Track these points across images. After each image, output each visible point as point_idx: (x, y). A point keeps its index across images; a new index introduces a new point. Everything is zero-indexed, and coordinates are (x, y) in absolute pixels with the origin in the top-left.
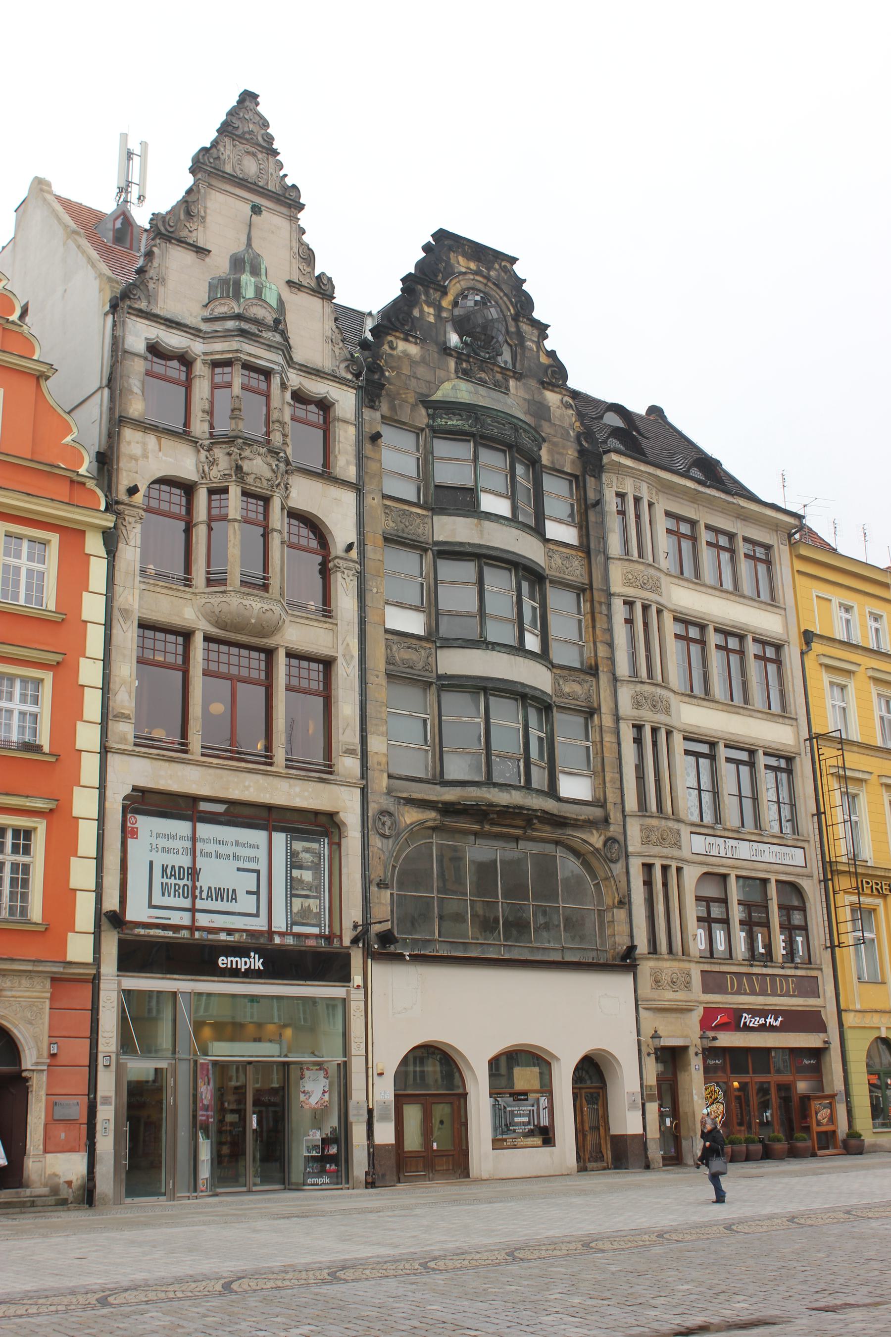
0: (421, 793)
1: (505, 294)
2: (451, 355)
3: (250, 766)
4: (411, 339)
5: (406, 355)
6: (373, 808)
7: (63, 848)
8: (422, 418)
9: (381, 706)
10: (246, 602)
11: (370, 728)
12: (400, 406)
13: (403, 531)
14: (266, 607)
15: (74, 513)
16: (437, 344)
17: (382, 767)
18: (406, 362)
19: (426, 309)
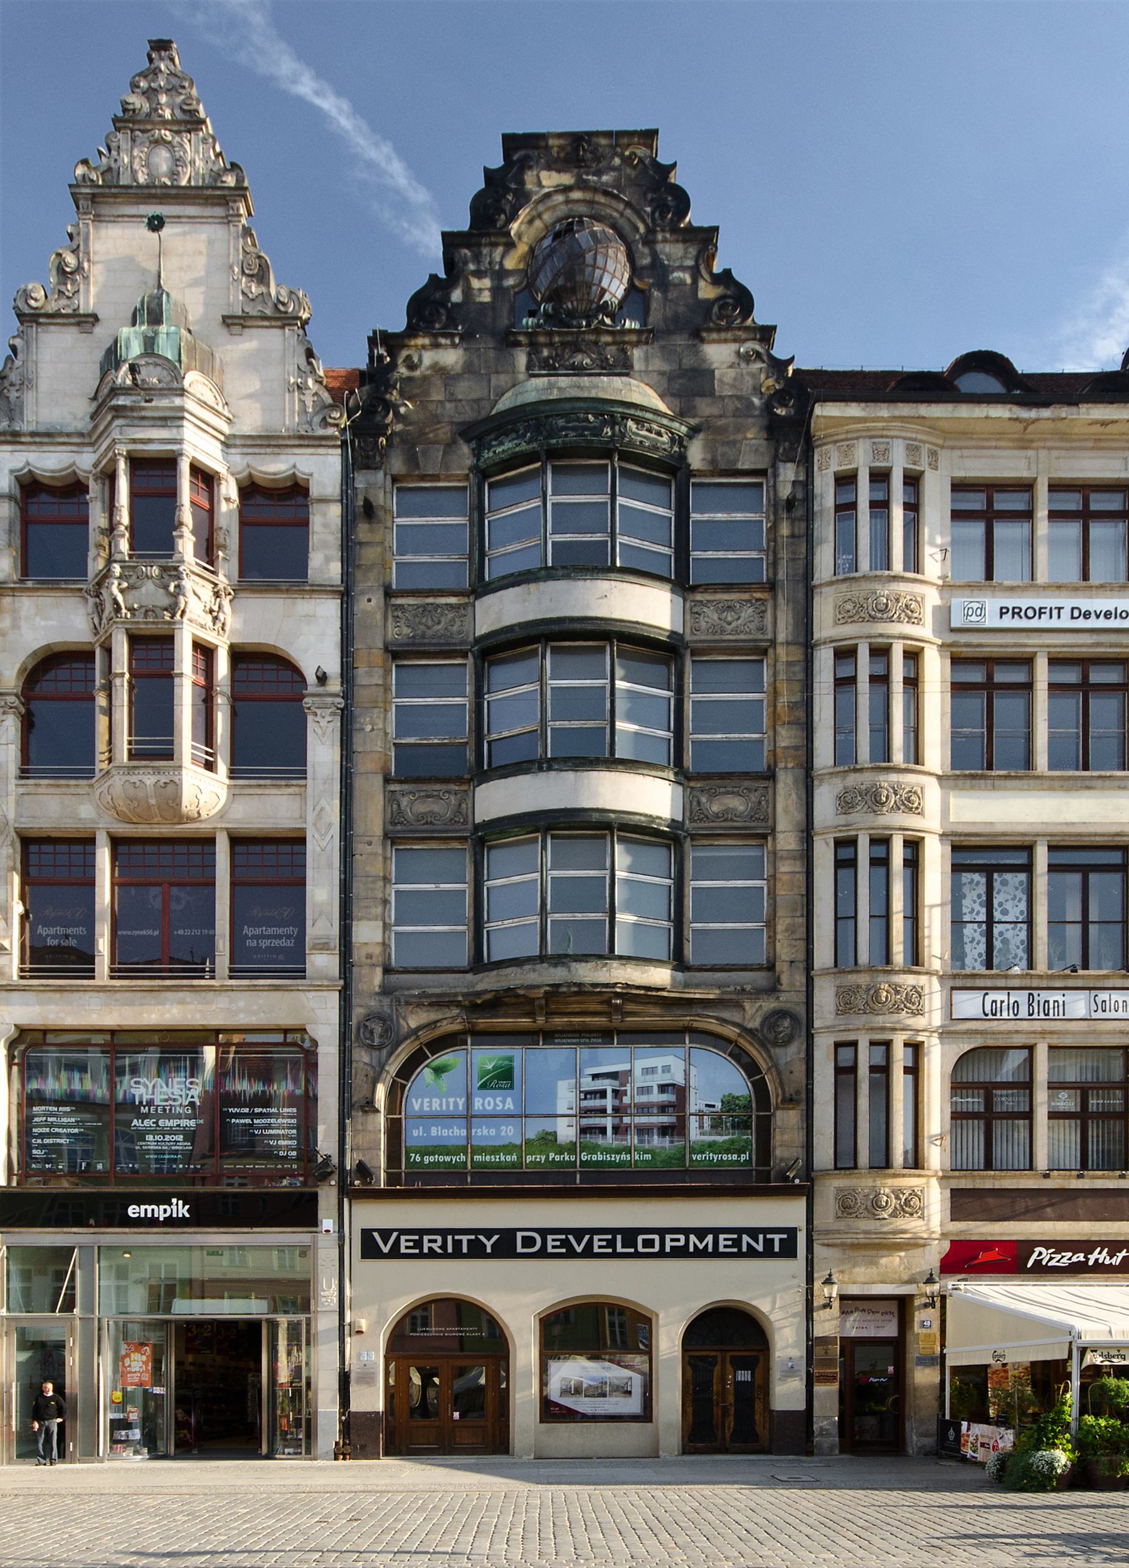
1: (628, 204)
2: (518, 344)
4: (443, 341)
5: (439, 370)
9: (374, 882)
10: (133, 779)
12: (424, 453)
13: (423, 636)
16: (493, 334)
17: (374, 960)
18: (438, 382)
19: (476, 283)
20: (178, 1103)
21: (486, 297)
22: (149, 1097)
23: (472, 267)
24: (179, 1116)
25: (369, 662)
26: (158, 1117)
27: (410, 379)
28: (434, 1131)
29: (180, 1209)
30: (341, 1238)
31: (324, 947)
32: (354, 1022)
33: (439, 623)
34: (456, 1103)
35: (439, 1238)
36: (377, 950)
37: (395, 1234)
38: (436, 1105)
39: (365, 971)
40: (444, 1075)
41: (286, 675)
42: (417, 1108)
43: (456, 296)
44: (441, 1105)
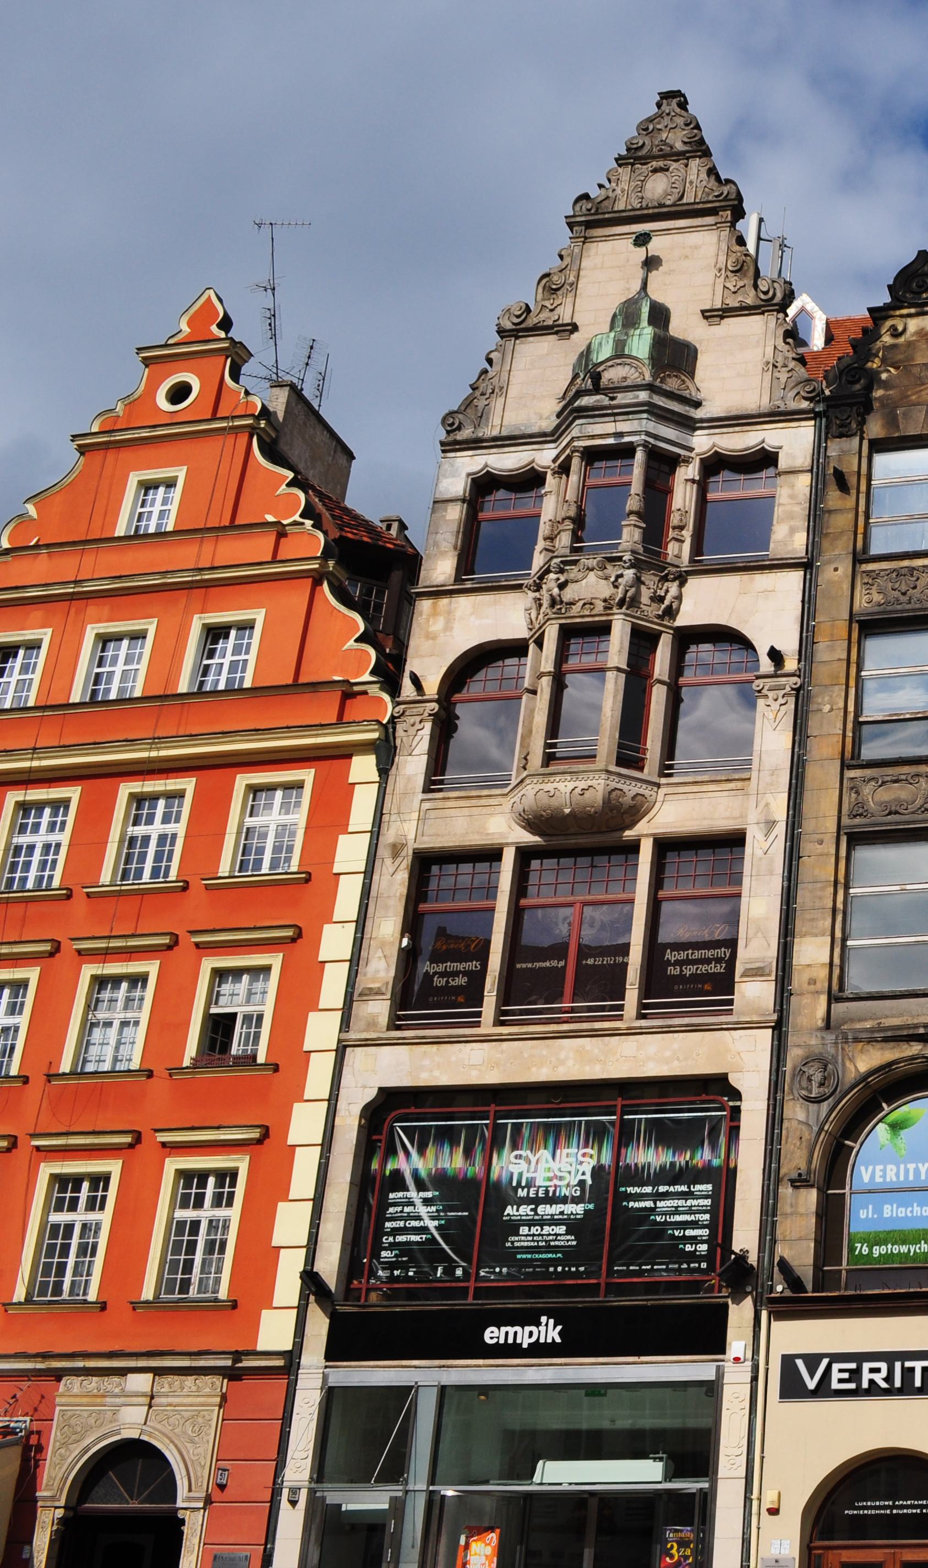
0: (901, 1015)
3: (565, 1027)
6: (794, 1055)
7: (271, 1188)
9: (822, 889)
11: (799, 926)
12: (904, 414)
14: (582, 785)
15: (317, 736)
20: (565, 1182)
22: (530, 1175)
24: (564, 1200)
25: (832, 635)
26: (537, 1201)
27: (894, 346)
28: (887, 1211)
29: (550, 1332)
30: (755, 1368)
31: (755, 973)
32: (788, 1068)
33: (915, 588)
34: (917, 1171)
35: (883, 1366)
36: (823, 973)
37: (825, 1362)
38: (891, 1175)
39: (806, 1000)
40: (903, 1132)
41: (738, 656)
42: (866, 1179)
44: (897, 1175)
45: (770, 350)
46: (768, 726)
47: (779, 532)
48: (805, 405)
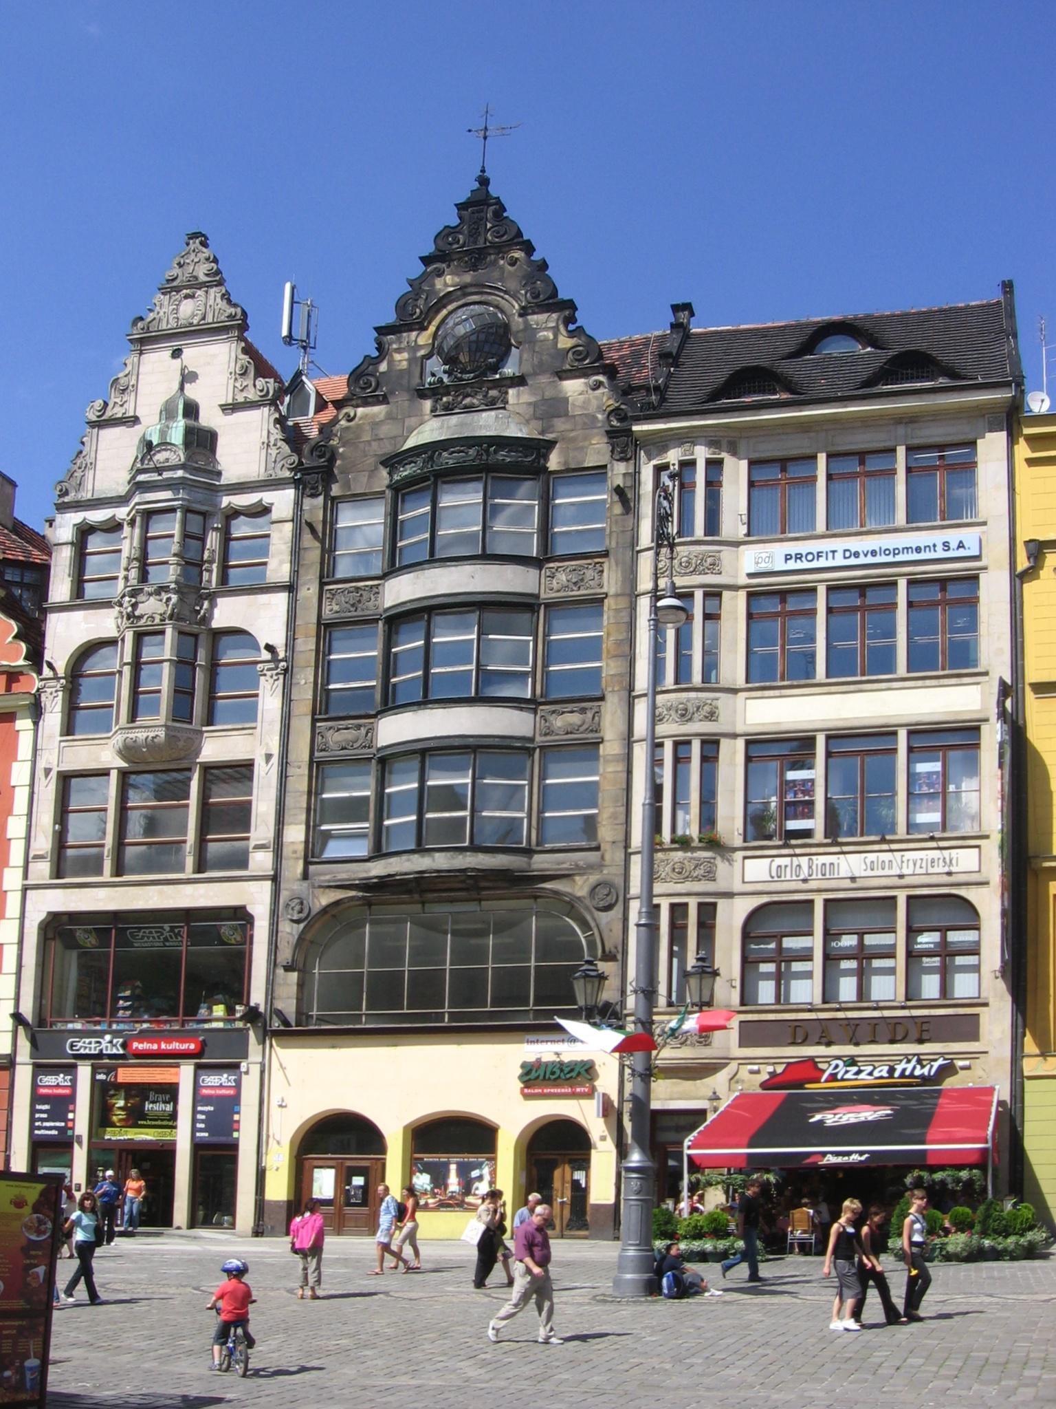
8: (383, 478)
16: (408, 390)
21: (404, 365)
23: (395, 346)
43: (383, 367)
45: (265, 433)
46: (268, 693)
47: (273, 563)
48: (288, 474)
